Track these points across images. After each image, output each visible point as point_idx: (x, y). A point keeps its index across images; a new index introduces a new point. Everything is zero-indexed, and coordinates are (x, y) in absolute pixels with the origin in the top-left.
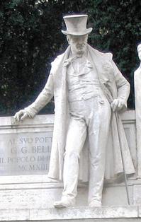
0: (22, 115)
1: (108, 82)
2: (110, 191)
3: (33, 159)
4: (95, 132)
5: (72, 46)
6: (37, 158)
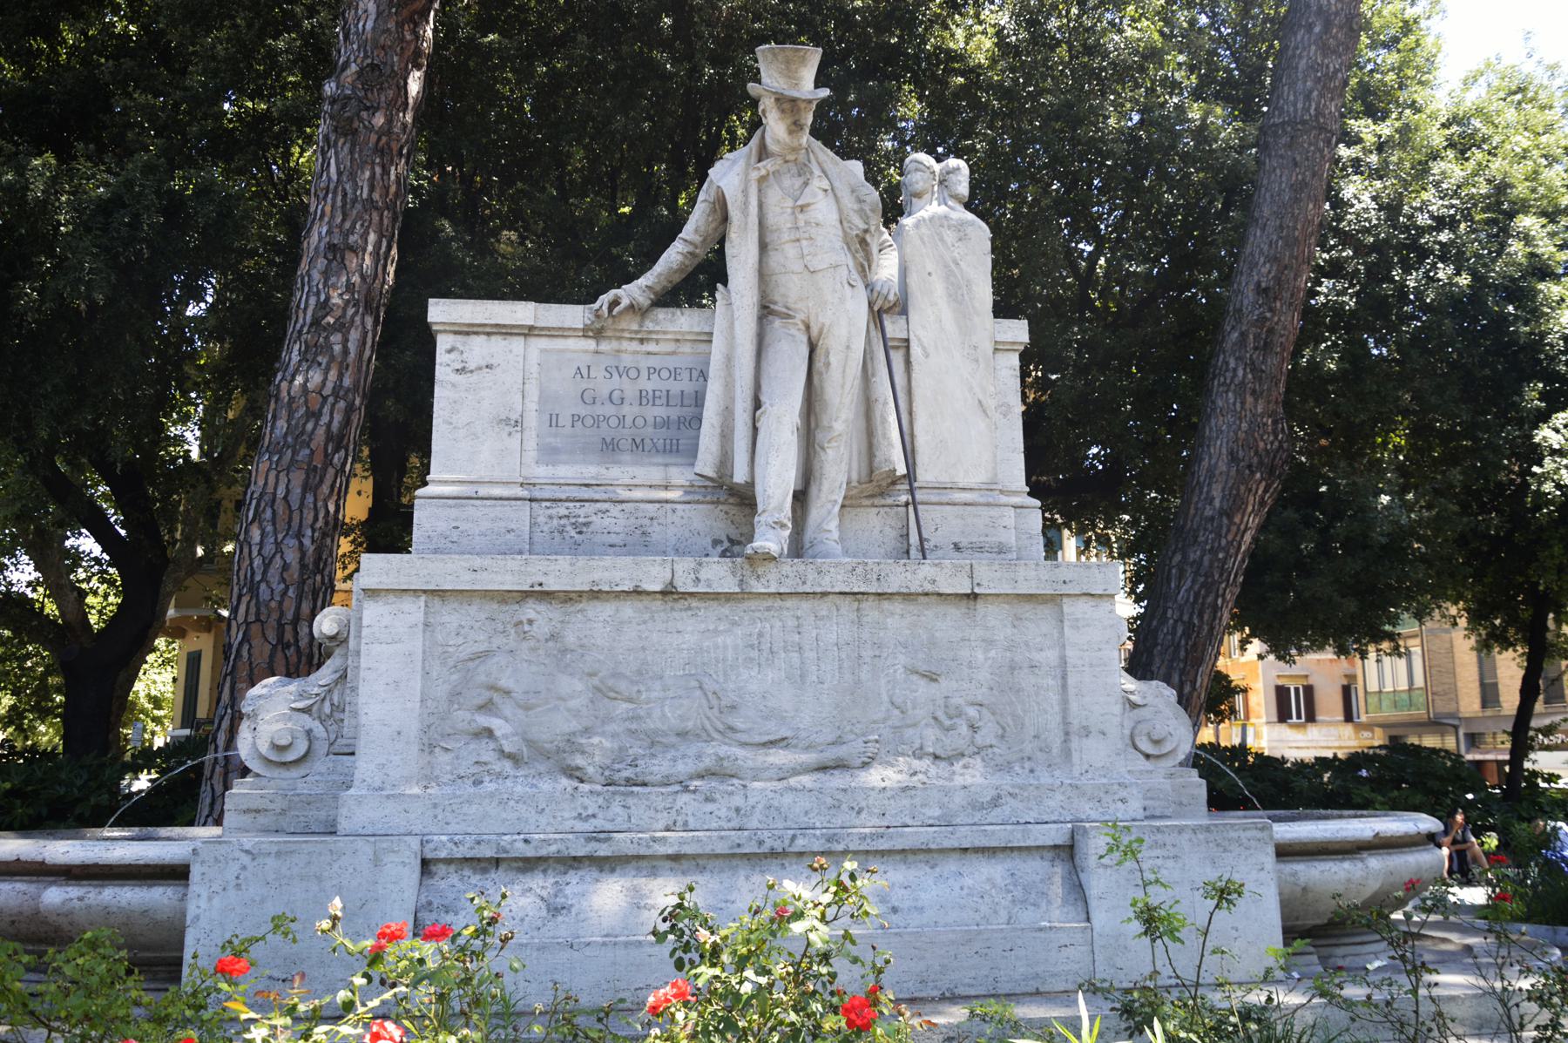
0: (615, 303)
1: (866, 231)
3: (640, 422)
4: (832, 359)
5: (775, 126)
6: (650, 420)
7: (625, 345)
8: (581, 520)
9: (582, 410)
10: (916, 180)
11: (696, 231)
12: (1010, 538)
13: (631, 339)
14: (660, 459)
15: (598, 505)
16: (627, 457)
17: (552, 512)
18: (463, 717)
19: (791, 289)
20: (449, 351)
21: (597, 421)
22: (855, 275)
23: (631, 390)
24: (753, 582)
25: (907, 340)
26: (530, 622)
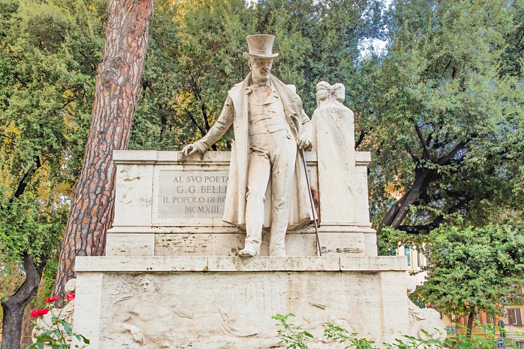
0: (190, 150)
2: (291, 237)
4: (280, 170)
6: (206, 199)
7: (196, 168)
8: (176, 242)
9: (178, 195)
10: (321, 93)
11: (224, 118)
12: (362, 247)
13: (198, 165)
14: (210, 215)
15: (184, 235)
16: (196, 214)
17: (164, 238)
18: (120, 325)
19: (261, 141)
20: (122, 172)
21: (183, 200)
22: (291, 133)
23: (198, 186)
24: (242, 266)
25: (317, 162)
26: (147, 284)
